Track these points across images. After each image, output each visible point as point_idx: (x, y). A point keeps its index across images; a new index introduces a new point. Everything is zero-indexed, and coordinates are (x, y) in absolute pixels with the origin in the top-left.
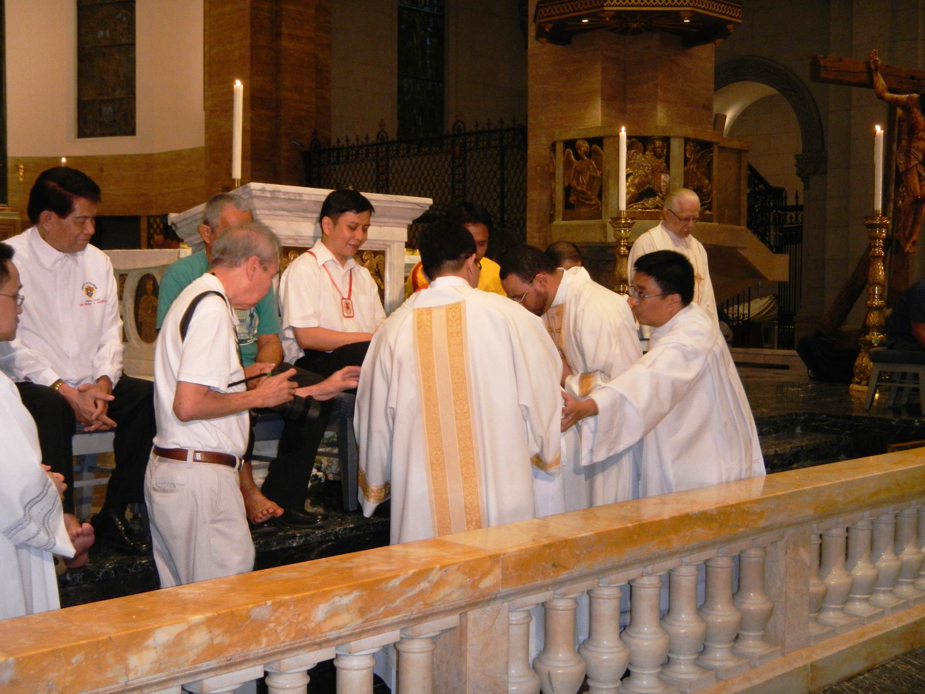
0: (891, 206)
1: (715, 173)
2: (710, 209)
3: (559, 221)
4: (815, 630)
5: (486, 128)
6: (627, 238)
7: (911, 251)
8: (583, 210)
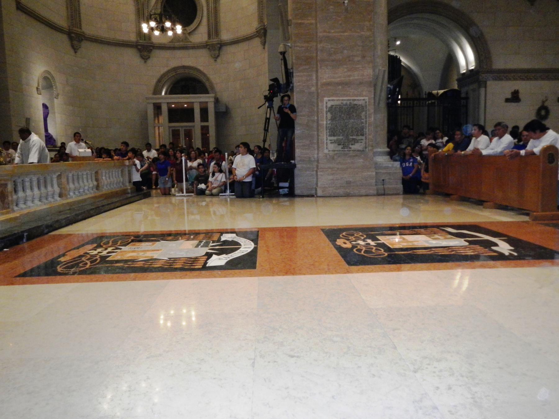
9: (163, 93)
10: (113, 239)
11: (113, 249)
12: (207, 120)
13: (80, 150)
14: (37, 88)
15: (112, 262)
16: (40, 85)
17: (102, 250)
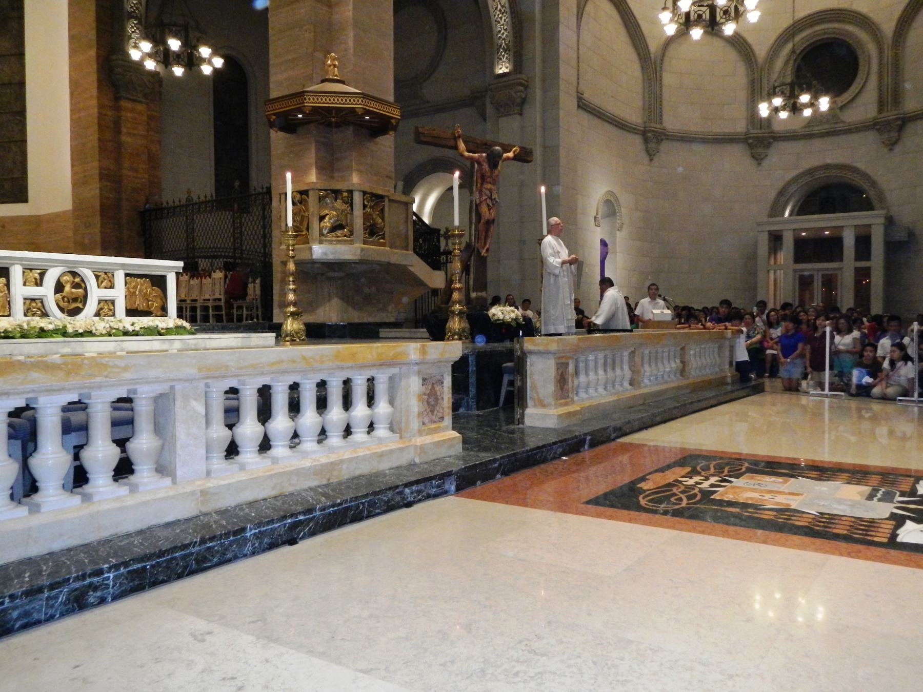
1: (386, 215)
2: (383, 239)
9: (787, 214)
10: (715, 463)
11: (718, 481)
13: (656, 311)
14: (595, 218)
15: (721, 503)
16: (600, 213)
17: (701, 480)
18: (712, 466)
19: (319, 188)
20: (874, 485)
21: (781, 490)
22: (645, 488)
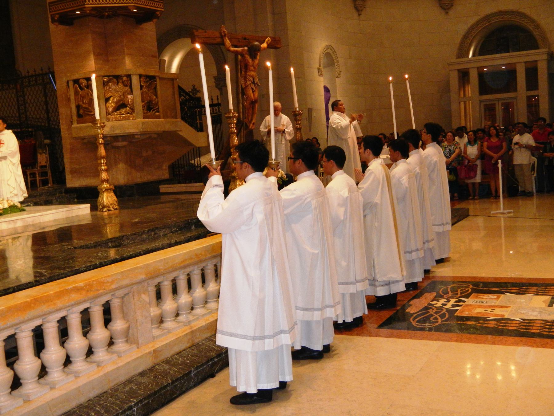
0: (241, 105)
2: (158, 112)
3: (75, 125)
4: (156, 332)
5: (34, 73)
6: (102, 134)
7: (253, 128)
8: (87, 118)
10: (450, 287)
11: (456, 302)
12: (536, 87)
14: (319, 69)
15: (462, 318)
16: (322, 65)
17: (445, 302)
18: (449, 290)
19: (103, 75)
20: (552, 294)
21: (496, 304)
22: (412, 312)
